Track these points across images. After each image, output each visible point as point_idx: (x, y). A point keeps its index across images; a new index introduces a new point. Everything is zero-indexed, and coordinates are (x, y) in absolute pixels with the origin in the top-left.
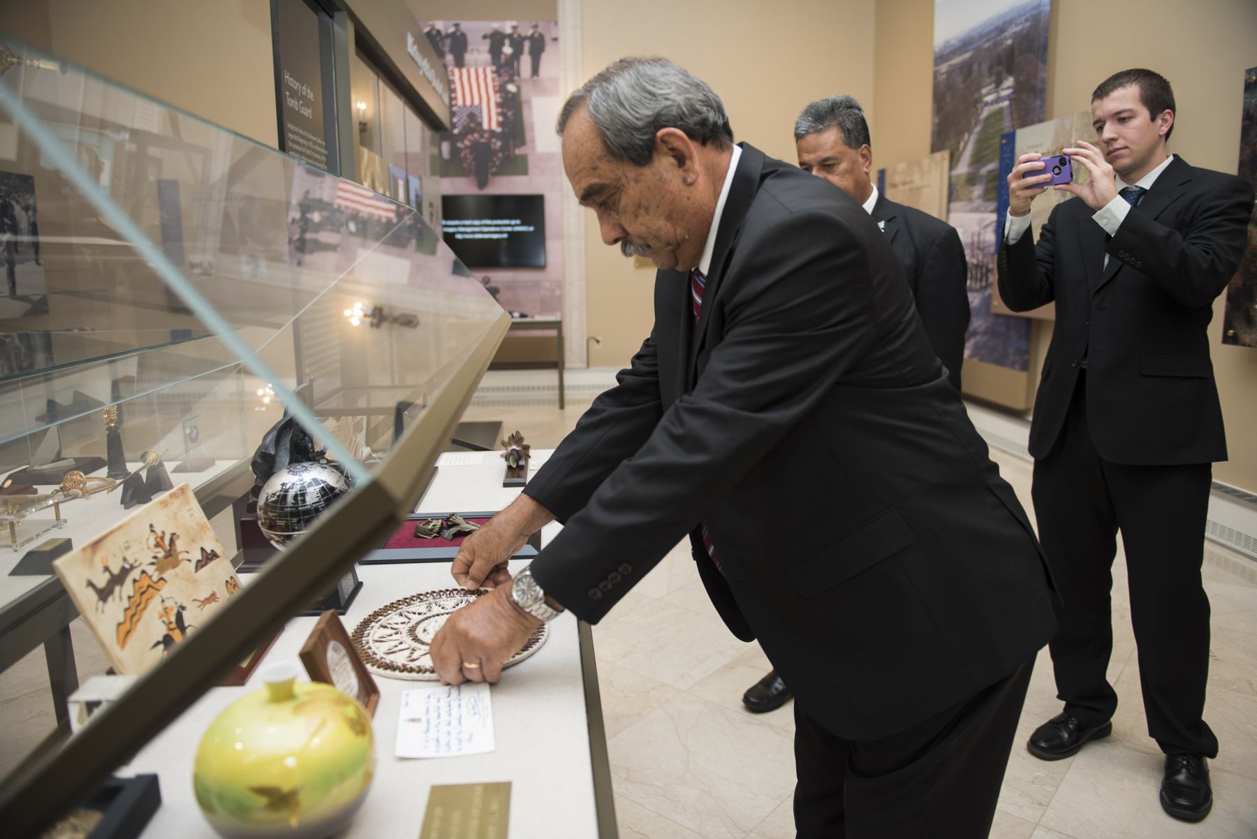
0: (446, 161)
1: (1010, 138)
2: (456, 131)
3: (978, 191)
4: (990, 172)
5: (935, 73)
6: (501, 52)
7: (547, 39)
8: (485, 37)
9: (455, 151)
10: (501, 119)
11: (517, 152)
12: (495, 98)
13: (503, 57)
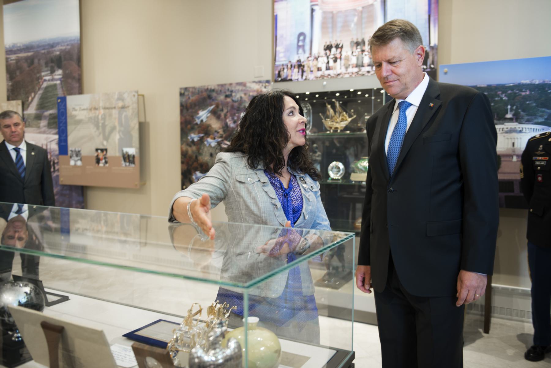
1: (64, 100)
3: (43, 123)
4: (50, 114)
5: (7, 59)
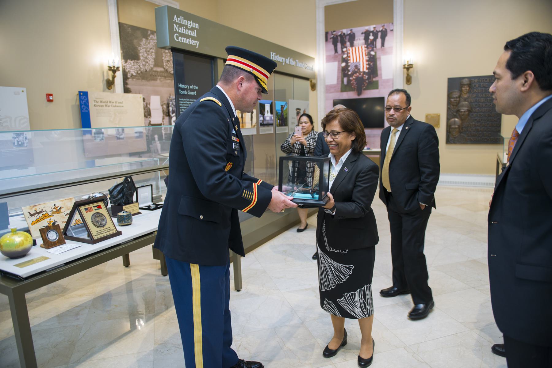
0: (346, 85)
2: (350, 73)
6: (369, 39)
7: (388, 31)
8: (362, 33)
9: (349, 81)
10: (368, 66)
11: (374, 79)
12: (366, 58)
13: (369, 41)
